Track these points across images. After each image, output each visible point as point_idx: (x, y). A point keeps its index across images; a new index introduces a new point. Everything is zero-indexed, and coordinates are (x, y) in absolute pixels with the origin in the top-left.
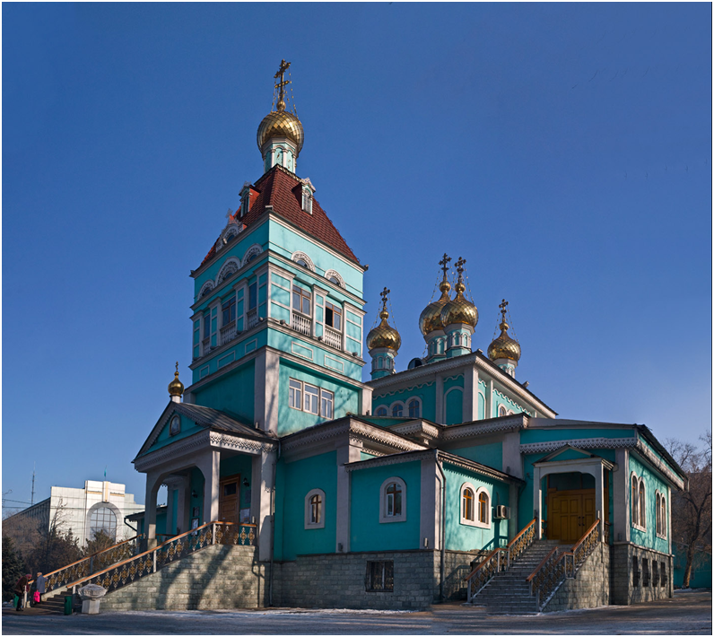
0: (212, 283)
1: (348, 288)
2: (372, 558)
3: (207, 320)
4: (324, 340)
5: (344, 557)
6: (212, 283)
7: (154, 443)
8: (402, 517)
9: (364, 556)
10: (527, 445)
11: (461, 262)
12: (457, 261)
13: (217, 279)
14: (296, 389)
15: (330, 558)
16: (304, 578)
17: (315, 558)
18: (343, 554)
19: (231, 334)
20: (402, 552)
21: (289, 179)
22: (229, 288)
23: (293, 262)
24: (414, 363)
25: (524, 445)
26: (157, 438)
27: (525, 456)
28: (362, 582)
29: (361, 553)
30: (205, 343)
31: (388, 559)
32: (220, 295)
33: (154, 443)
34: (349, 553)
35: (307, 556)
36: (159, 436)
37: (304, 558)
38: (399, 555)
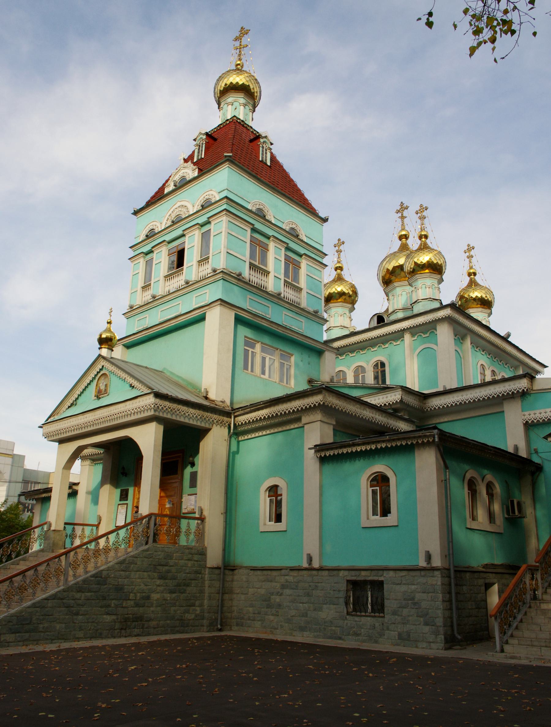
0: (158, 225)
1: (305, 239)
2: (352, 576)
3: (149, 264)
4: (282, 295)
5: (314, 572)
6: (158, 225)
7: (72, 405)
8: (391, 519)
9: (341, 573)
10: (532, 412)
11: (423, 209)
12: (418, 208)
13: (165, 221)
14: (286, 363)
15: (295, 573)
16: (263, 591)
17: (275, 573)
18: (314, 569)
19: (178, 282)
20: (395, 570)
21: (245, 130)
22: (179, 232)
23: (250, 211)
24: (375, 318)
25: (526, 413)
26: (77, 399)
27: (528, 426)
28: (342, 601)
29: (338, 569)
30: (146, 287)
31: (376, 578)
32: (168, 238)
33: (72, 405)
34: (321, 569)
35: (263, 569)
36: (79, 395)
37: (259, 572)
38: (391, 573)
